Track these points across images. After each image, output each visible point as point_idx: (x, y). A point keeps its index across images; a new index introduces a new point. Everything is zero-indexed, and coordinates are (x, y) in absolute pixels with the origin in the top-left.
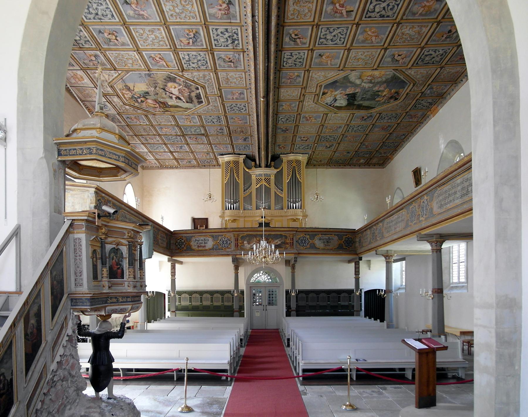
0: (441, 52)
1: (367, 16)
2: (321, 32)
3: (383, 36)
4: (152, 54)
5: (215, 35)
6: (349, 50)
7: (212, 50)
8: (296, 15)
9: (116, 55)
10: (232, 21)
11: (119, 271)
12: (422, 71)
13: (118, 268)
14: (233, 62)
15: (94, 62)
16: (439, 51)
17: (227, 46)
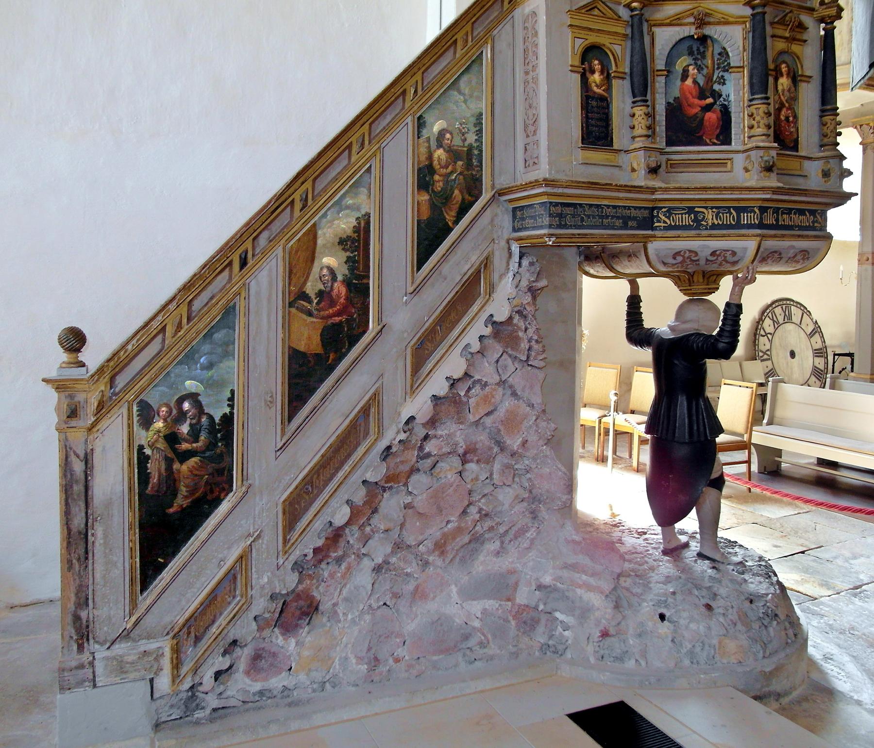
11: (712, 117)
13: (708, 108)
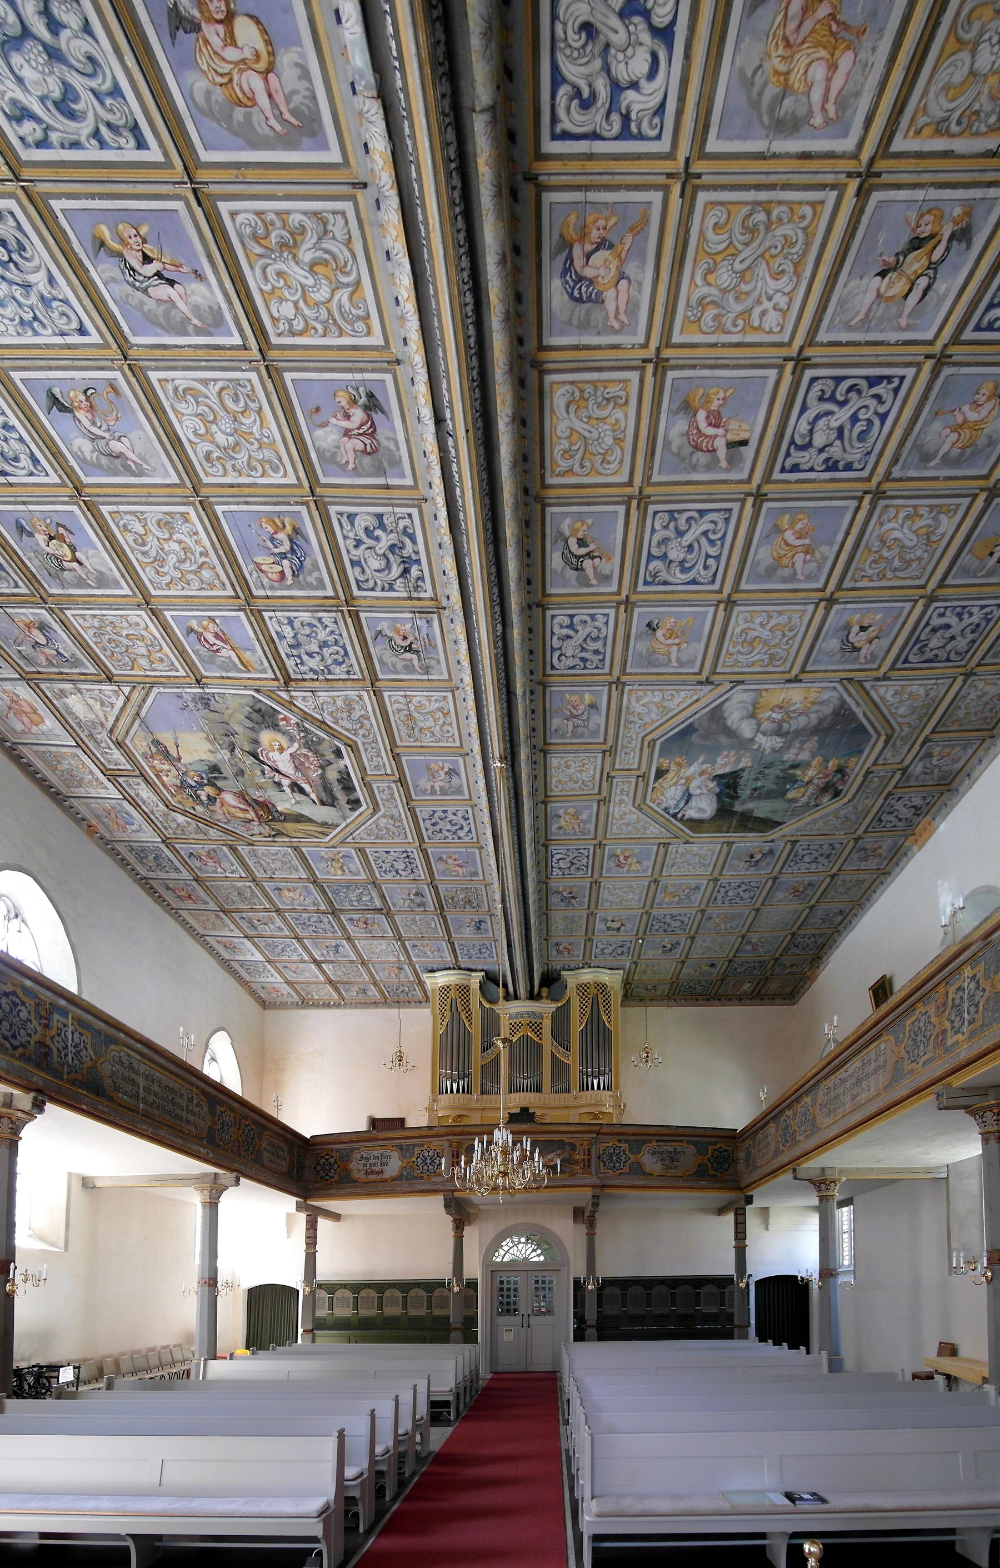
0: (975, 619)
1: (788, 464)
2: (653, 530)
3: (824, 549)
4: (194, 617)
5: (351, 543)
6: (730, 604)
7: (350, 599)
8: (578, 457)
9: (96, 623)
10: (393, 481)
12: (914, 688)
14: (417, 652)
15: (47, 651)
16: (971, 614)
17: (391, 588)
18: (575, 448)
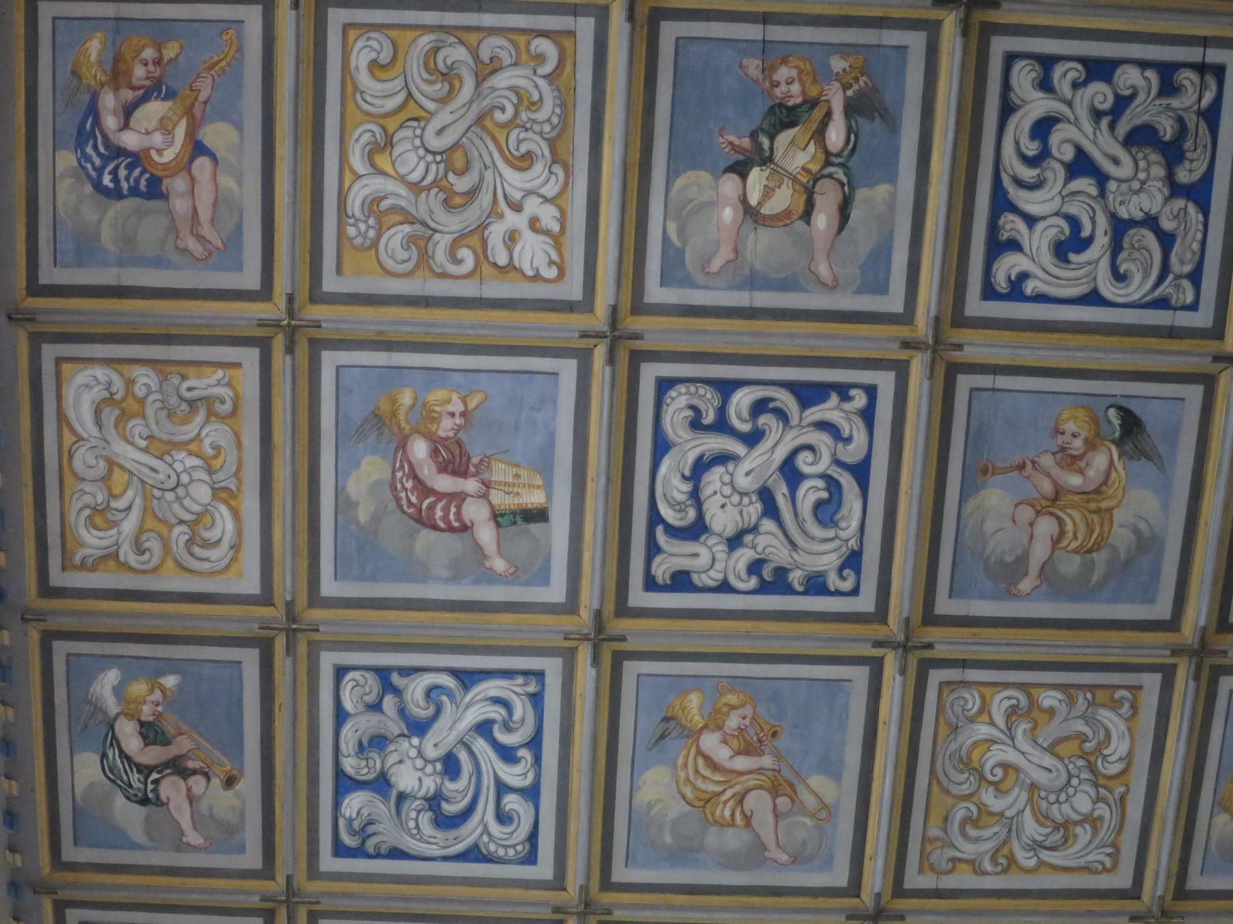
18: (121, 504)
